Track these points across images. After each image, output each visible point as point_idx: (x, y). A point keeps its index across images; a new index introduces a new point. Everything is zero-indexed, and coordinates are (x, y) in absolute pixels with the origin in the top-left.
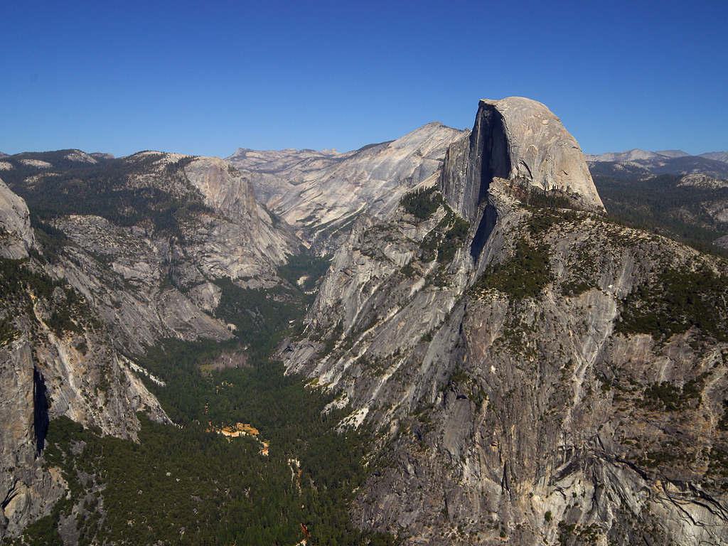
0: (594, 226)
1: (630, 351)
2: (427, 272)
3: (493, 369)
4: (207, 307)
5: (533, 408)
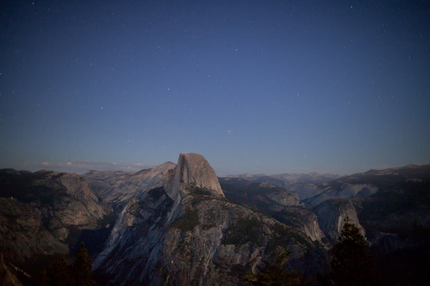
0: (216, 202)
1: (226, 252)
2: (157, 221)
3: (172, 262)
4: (61, 238)
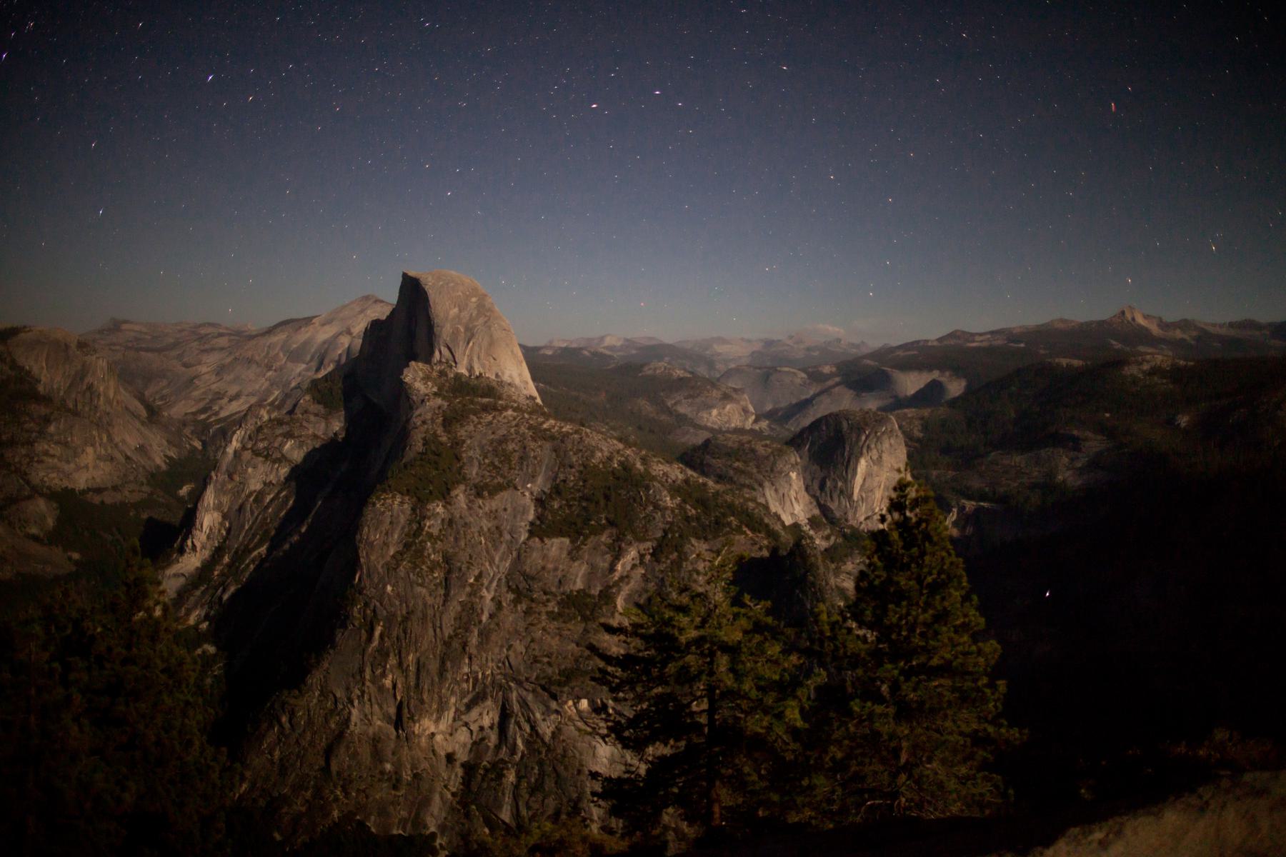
0: (515, 419)
1: (545, 557)
3: (389, 588)
4: (34, 530)
5: (435, 631)
